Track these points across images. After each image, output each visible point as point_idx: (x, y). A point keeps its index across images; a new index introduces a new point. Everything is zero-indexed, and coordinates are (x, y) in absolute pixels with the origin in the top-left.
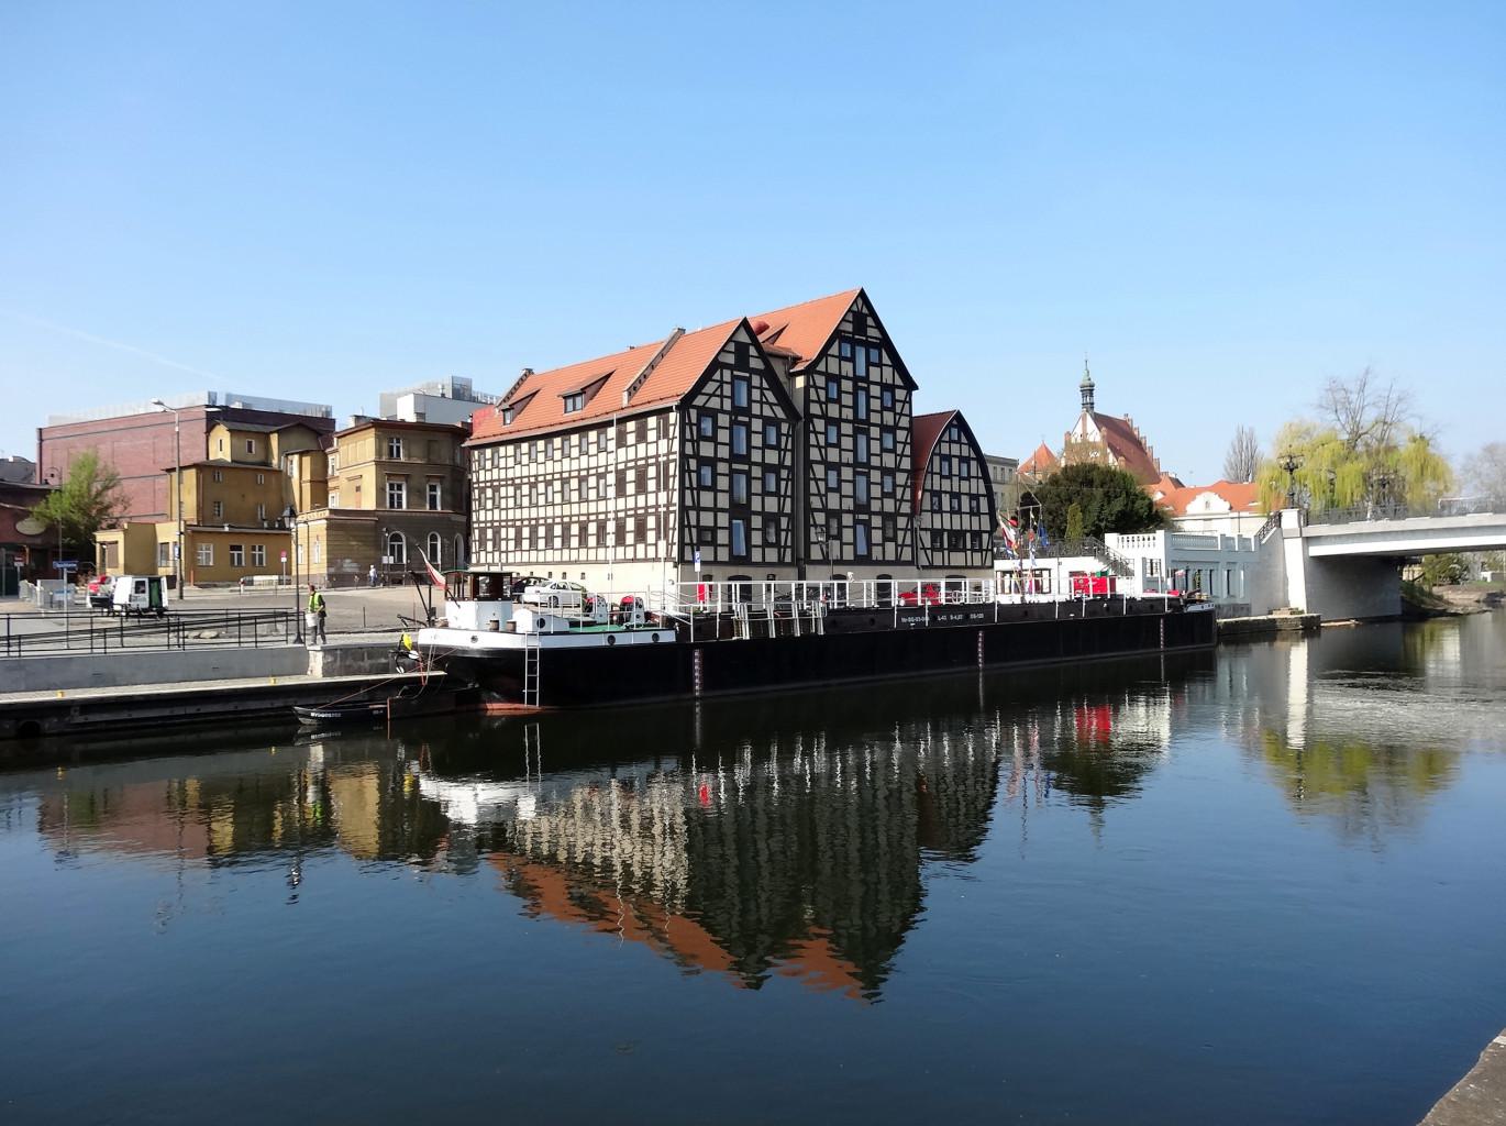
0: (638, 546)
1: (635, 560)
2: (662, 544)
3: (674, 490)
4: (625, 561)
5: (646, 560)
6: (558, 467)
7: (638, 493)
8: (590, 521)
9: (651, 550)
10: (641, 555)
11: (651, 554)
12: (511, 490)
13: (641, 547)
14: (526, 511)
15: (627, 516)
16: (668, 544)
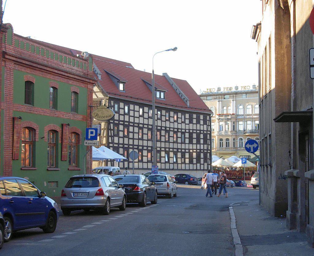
0: (198, 164)
1: (197, 170)
2: (206, 164)
3: (209, 145)
4: (193, 170)
5: (200, 170)
6: (187, 127)
7: (196, 144)
8: (179, 152)
9: (202, 166)
10: (198, 168)
11: (202, 168)
12: (136, 130)
13: (198, 165)
14: (187, 145)
15: (193, 152)
16: (207, 165)
